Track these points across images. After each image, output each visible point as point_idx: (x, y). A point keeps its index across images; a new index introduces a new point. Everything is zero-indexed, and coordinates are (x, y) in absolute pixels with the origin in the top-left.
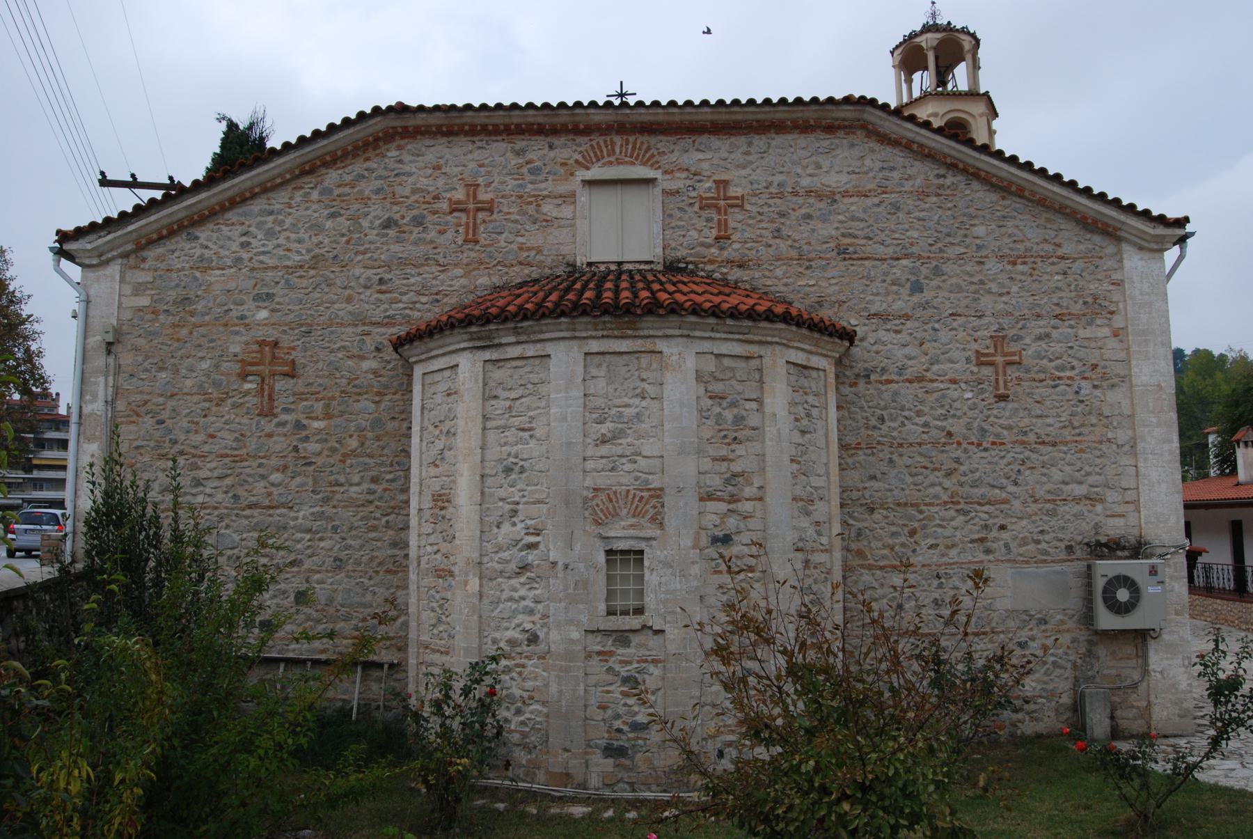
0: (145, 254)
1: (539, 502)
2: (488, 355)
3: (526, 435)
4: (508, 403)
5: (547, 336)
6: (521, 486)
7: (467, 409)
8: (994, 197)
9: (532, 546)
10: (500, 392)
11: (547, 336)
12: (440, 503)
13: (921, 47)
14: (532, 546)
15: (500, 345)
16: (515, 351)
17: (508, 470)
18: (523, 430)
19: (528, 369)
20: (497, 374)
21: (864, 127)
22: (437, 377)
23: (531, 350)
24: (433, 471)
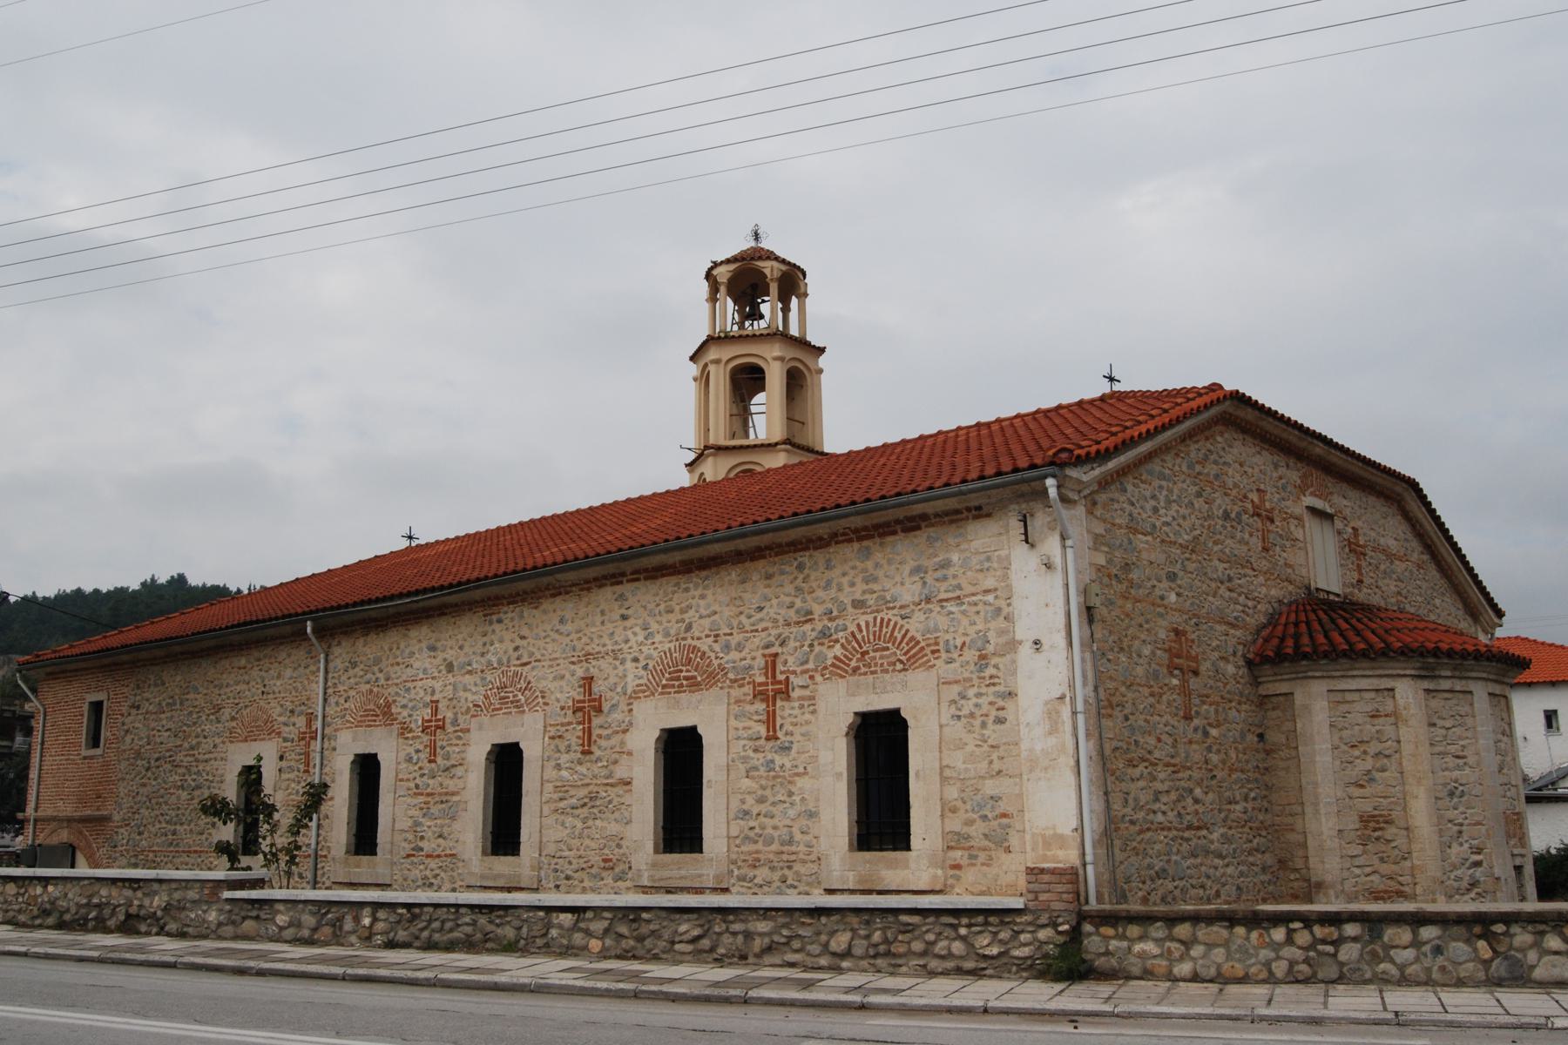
0: (1097, 497)
1: (1479, 823)
2: (1426, 684)
3: (1461, 762)
4: (1444, 732)
5: (1474, 674)
6: (1461, 809)
7: (1413, 735)
8: (1438, 575)
9: (1477, 864)
10: (1440, 723)
11: (1474, 674)
12: (1372, 824)
13: (765, 276)
14: (1477, 864)
15: (1441, 677)
16: (1446, 684)
17: (1451, 794)
18: (1458, 757)
19: (1454, 701)
20: (1435, 703)
21: (1399, 502)
22: (1349, 697)
23: (1459, 685)
24: (1357, 792)
